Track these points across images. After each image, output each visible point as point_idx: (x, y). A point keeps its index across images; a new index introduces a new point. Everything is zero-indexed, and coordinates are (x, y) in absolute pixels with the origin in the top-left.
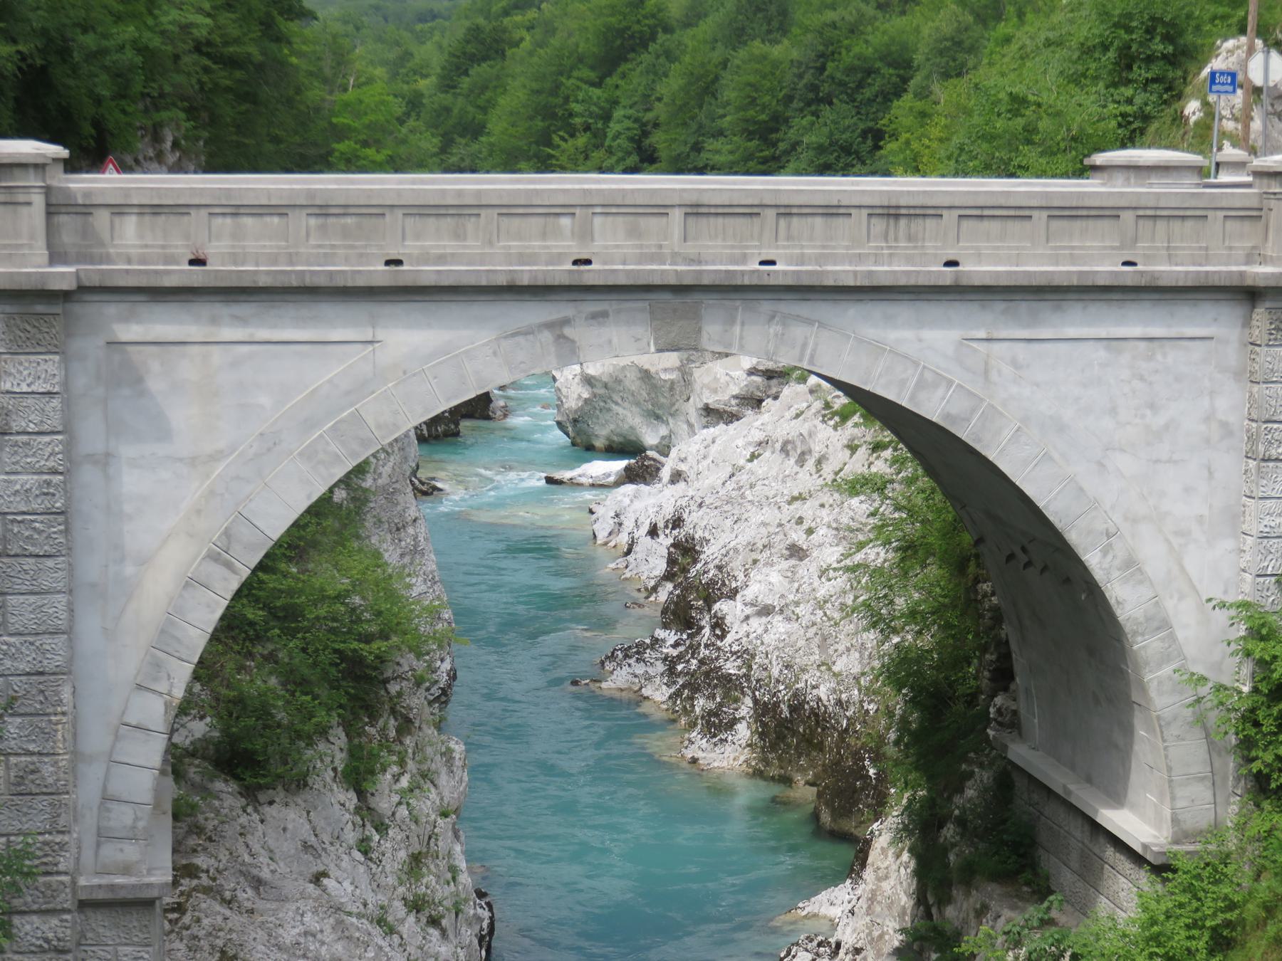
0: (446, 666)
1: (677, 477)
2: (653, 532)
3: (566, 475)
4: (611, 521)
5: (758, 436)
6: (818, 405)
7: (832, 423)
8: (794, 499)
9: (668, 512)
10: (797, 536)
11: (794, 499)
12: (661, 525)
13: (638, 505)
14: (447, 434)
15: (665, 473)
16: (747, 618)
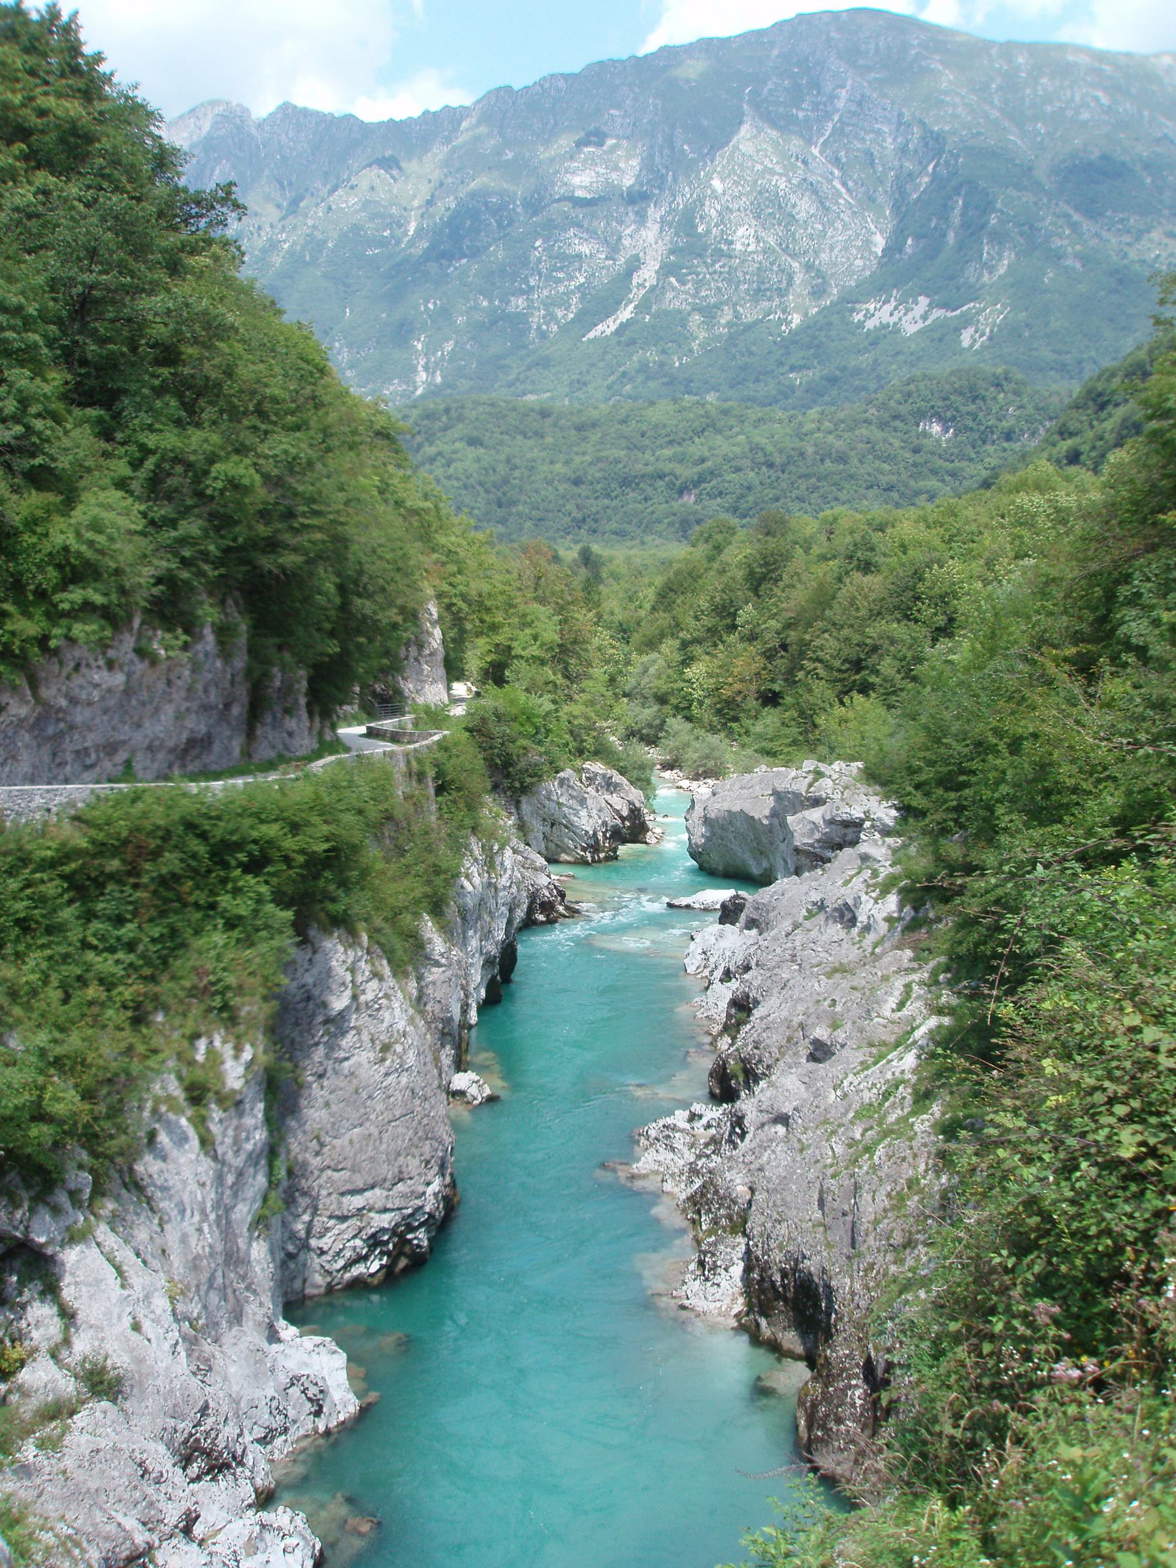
0: (435, 1186)
1: (751, 924)
2: (727, 975)
3: (683, 901)
4: (699, 957)
5: (815, 897)
6: (867, 873)
7: (874, 895)
8: (835, 970)
9: (739, 959)
10: (821, 1032)
11: (835, 970)
12: (732, 969)
13: (723, 944)
14: (608, 859)
15: (743, 917)
16: (763, 1125)
